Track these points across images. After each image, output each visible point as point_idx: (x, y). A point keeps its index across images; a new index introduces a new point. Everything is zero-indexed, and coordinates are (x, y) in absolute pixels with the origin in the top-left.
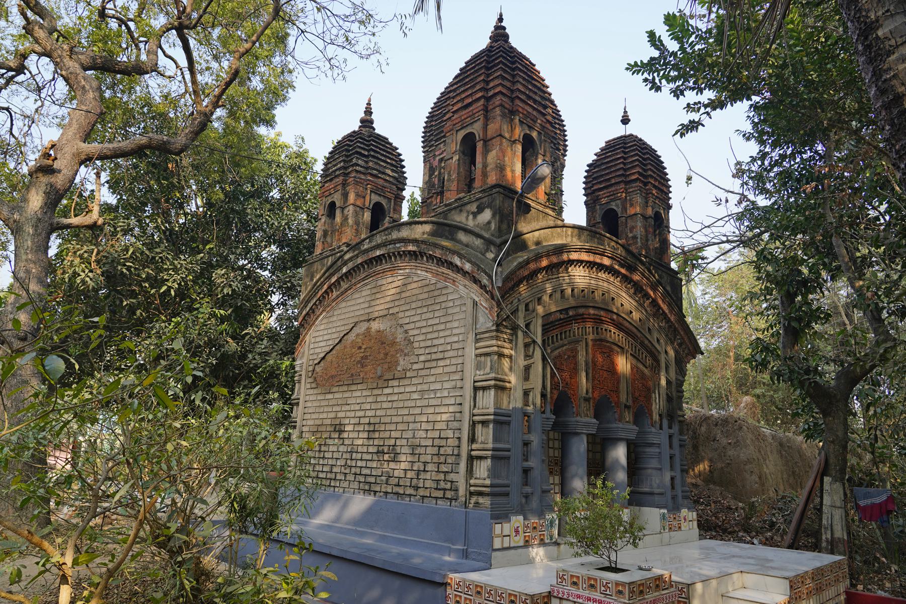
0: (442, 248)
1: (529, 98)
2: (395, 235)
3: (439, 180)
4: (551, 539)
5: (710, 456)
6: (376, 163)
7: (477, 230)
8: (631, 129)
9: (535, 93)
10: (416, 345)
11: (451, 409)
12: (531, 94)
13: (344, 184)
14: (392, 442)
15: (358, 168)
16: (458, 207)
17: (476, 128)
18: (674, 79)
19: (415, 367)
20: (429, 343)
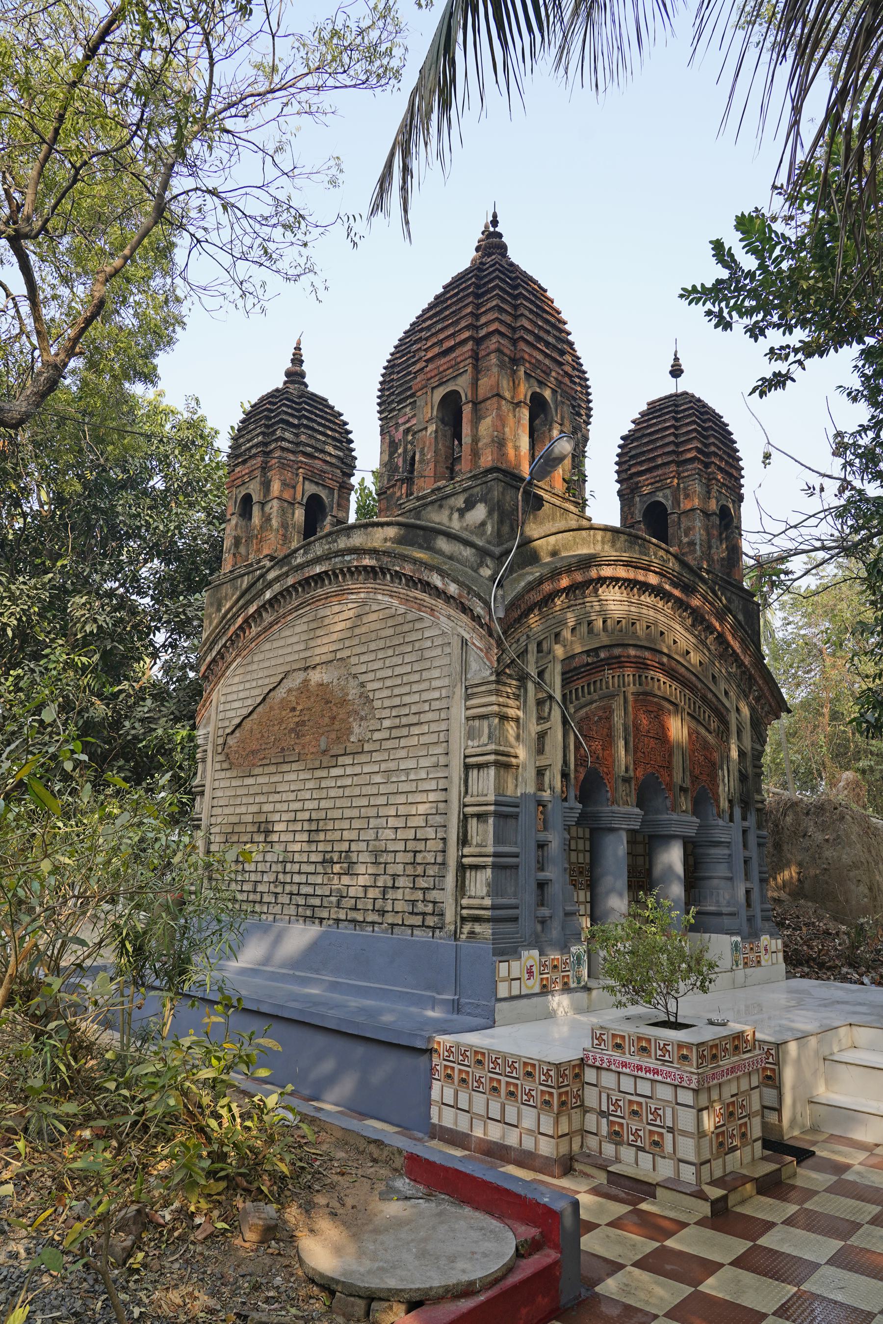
0: (415, 561)
1: (539, 339)
2: (343, 543)
3: (405, 461)
4: (579, 983)
5: (799, 858)
6: (310, 436)
7: (465, 535)
8: (684, 385)
9: (548, 332)
10: (377, 704)
11: (432, 797)
12: (542, 334)
13: (265, 468)
14: (345, 846)
15: (284, 444)
16: (436, 501)
17: (462, 385)
18: (750, 312)
19: (377, 736)
20: (397, 701)
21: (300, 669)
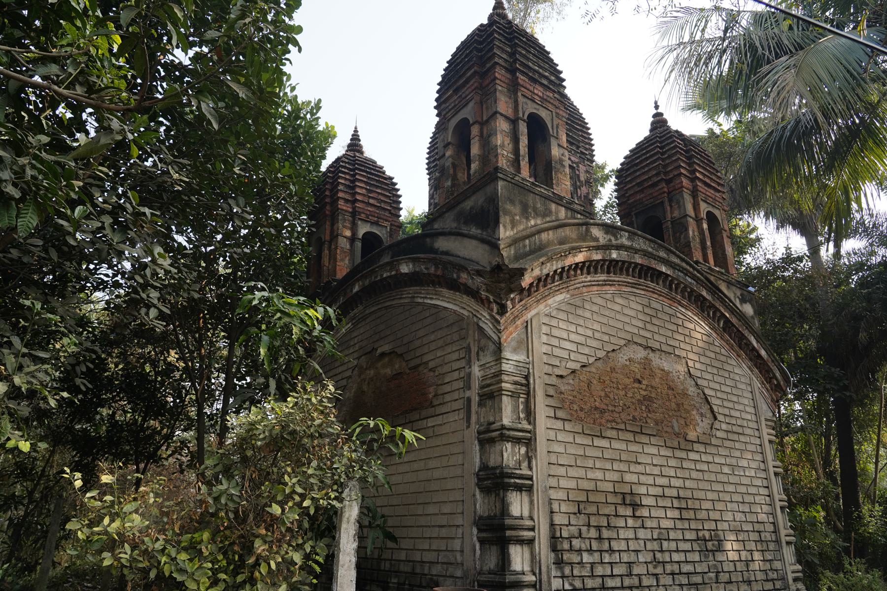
14: (713, 526)
21: (641, 345)
